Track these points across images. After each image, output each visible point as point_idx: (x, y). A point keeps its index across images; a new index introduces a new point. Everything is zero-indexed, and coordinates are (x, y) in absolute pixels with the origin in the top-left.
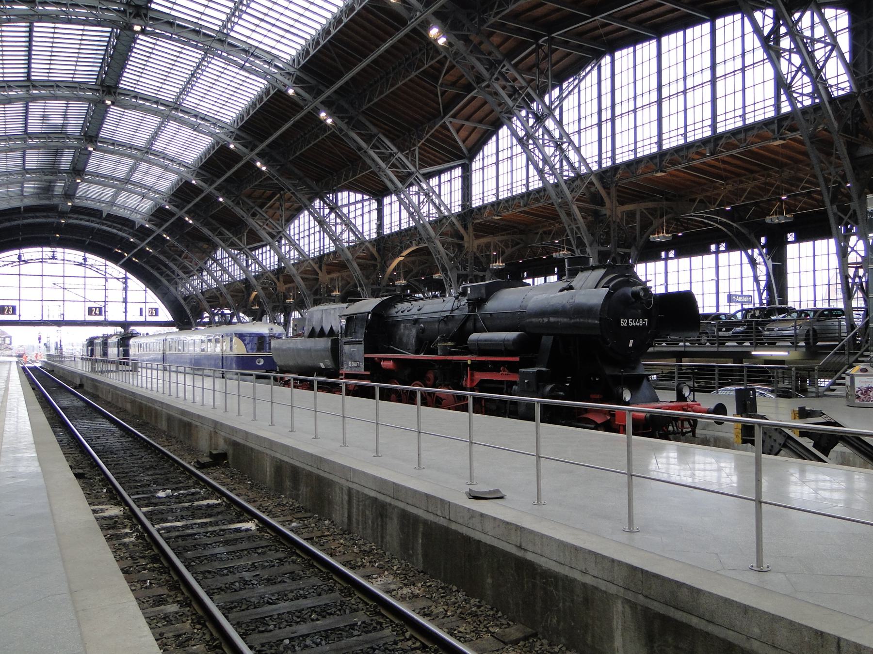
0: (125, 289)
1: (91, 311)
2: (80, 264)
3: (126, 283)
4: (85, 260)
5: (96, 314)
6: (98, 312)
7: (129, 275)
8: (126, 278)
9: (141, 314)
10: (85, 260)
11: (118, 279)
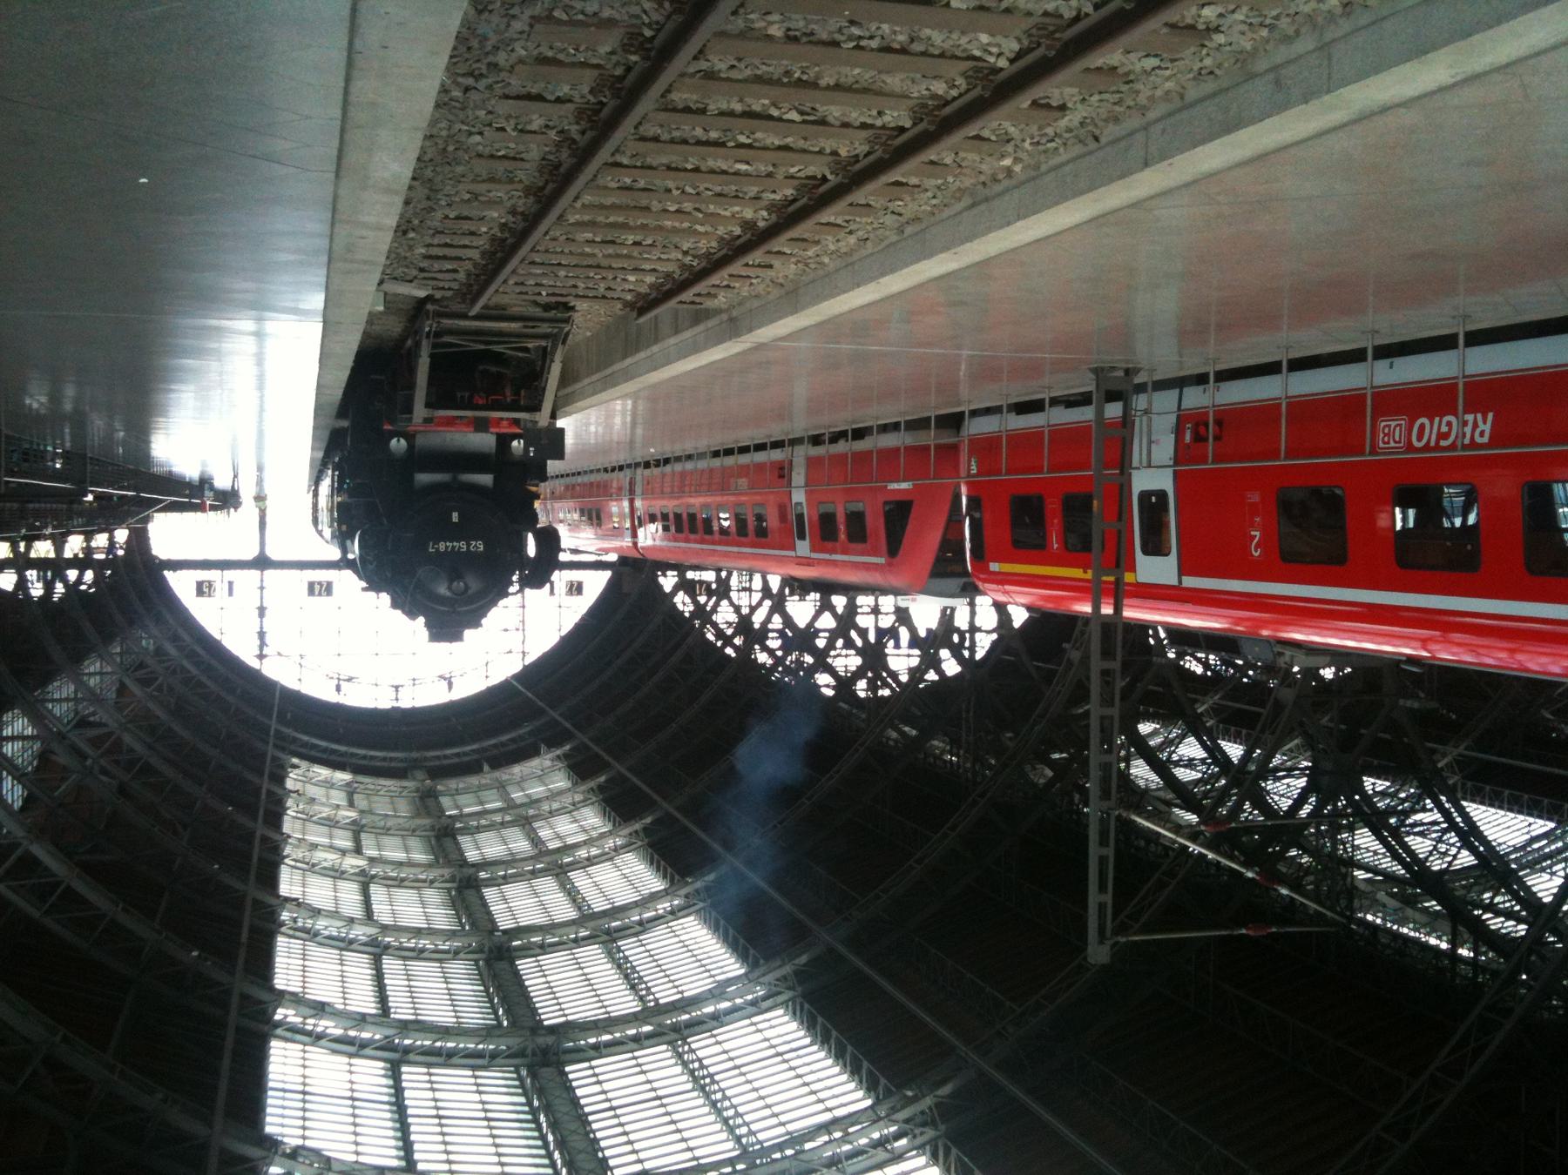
0: (262, 635)
1: (328, 589)
2: (350, 680)
3: (262, 644)
4: (338, 689)
5: (320, 583)
6: (317, 587)
7: (254, 663)
8: (261, 657)
9: (231, 584)
10: (338, 689)
11: (279, 654)
